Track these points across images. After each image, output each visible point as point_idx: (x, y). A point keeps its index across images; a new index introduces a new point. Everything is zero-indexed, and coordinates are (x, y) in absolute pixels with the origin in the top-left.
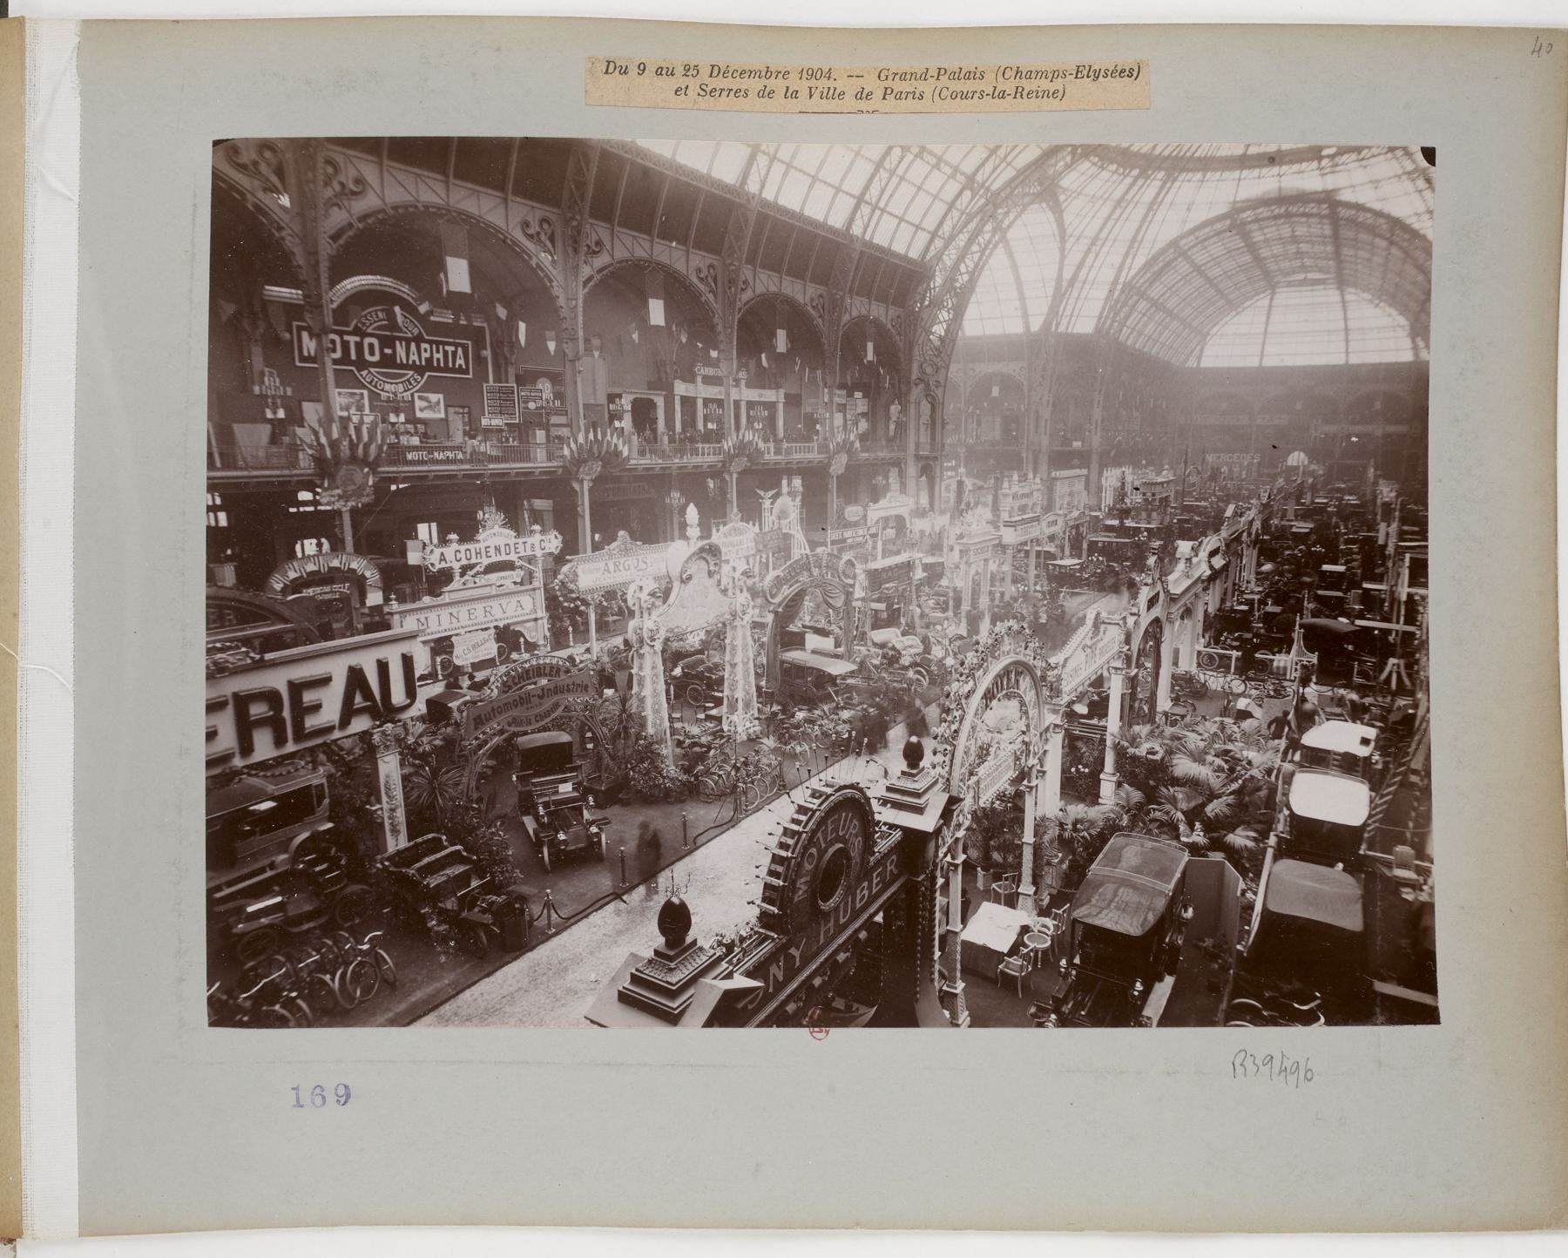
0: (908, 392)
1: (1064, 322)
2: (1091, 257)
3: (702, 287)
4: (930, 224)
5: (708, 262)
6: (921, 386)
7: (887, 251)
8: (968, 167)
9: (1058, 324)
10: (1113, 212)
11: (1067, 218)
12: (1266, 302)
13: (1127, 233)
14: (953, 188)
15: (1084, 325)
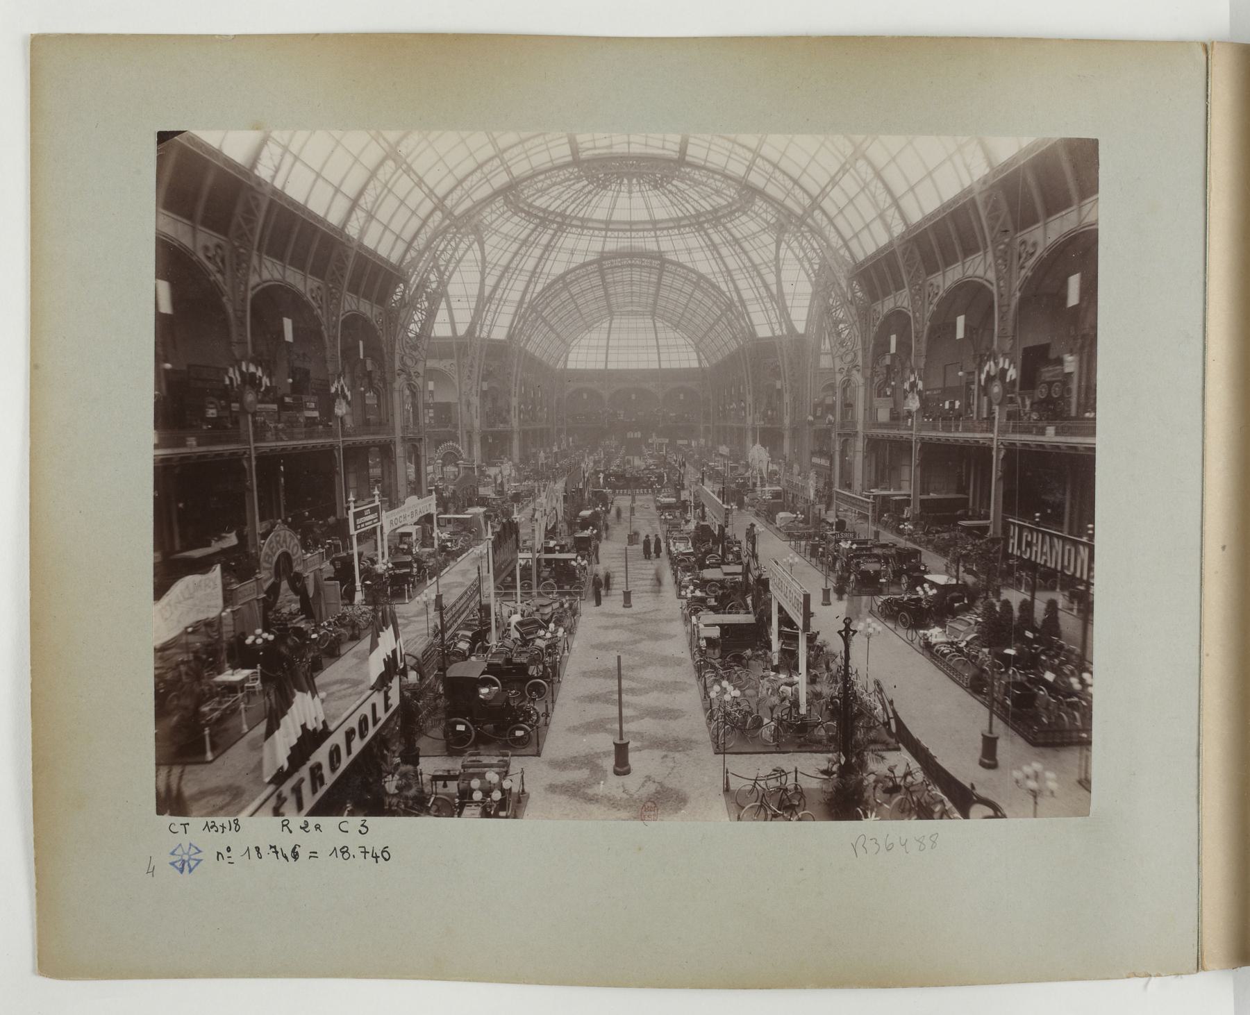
0: (394, 380)
1: (486, 329)
2: (504, 282)
3: (210, 266)
4: (407, 235)
5: (215, 241)
6: (403, 376)
7: (374, 253)
8: (440, 192)
10: (520, 248)
11: (487, 248)
12: (606, 325)
13: (530, 264)
14: (428, 205)
15: (500, 334)
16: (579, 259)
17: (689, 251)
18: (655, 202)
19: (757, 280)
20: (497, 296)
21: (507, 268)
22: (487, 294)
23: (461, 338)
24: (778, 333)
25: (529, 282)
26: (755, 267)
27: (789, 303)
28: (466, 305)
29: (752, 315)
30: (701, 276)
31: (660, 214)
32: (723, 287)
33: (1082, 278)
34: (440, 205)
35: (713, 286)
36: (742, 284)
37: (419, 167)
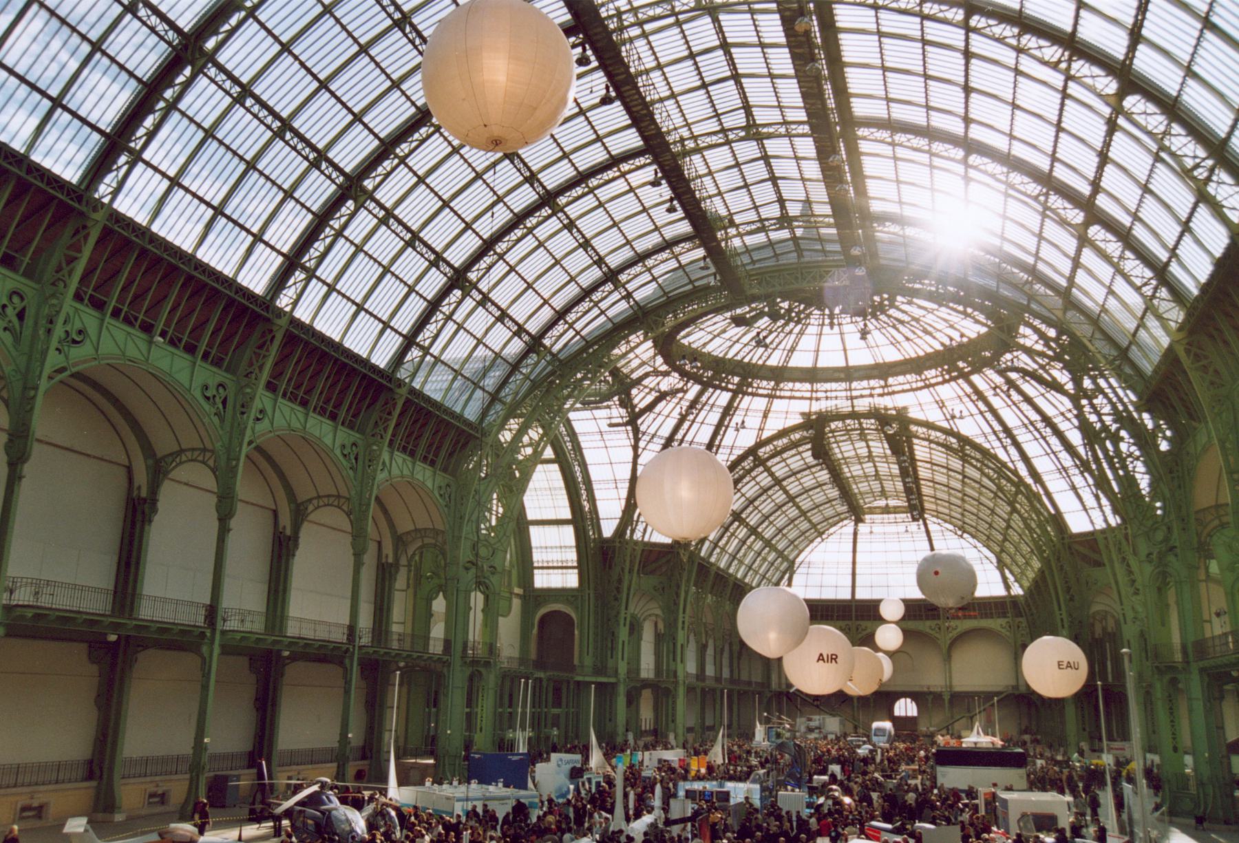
1: (640, 527)
8: (533, 327)
9: (633, 531)
14: (517, 346)
16: (774, 425)
19: (1054, 441)
23: (607, 540)
24: (1100, 525)
26: (1047, 420)
29: (1056, 497)
30: (964, 440)
31: (891, 355)
32: (1002, 455)
33: (522, 147)
34: (535, 344)
35: (985, 453)
36: (1032, 449)
37: (501, 296)
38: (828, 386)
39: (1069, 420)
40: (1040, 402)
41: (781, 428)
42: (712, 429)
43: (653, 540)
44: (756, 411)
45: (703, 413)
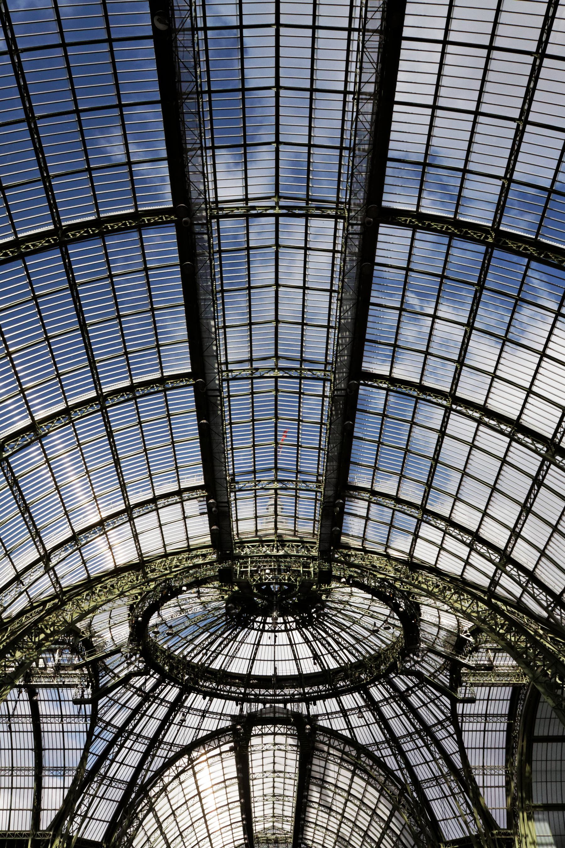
1: (78, 820)
16: (210, 724)
17: (344, 712)
18: (304, 651)
20: (102, 771)
21: (121, 730)
22: (89, 766)
23: (44, 833)
25: (146, 755)
26: (427, 729)
27: (479, 780)
28: (58, 782)
30: (362, 749)
31: (309, 667)
32: (391, 763)
36: (414, 758)
38: (257, 691)
39: (445, 728)
40: (423, 712)
41: (214, 729)
42: (158, 723)
43: (85, 837)
44: (197, 710)
45: (154, 706)
